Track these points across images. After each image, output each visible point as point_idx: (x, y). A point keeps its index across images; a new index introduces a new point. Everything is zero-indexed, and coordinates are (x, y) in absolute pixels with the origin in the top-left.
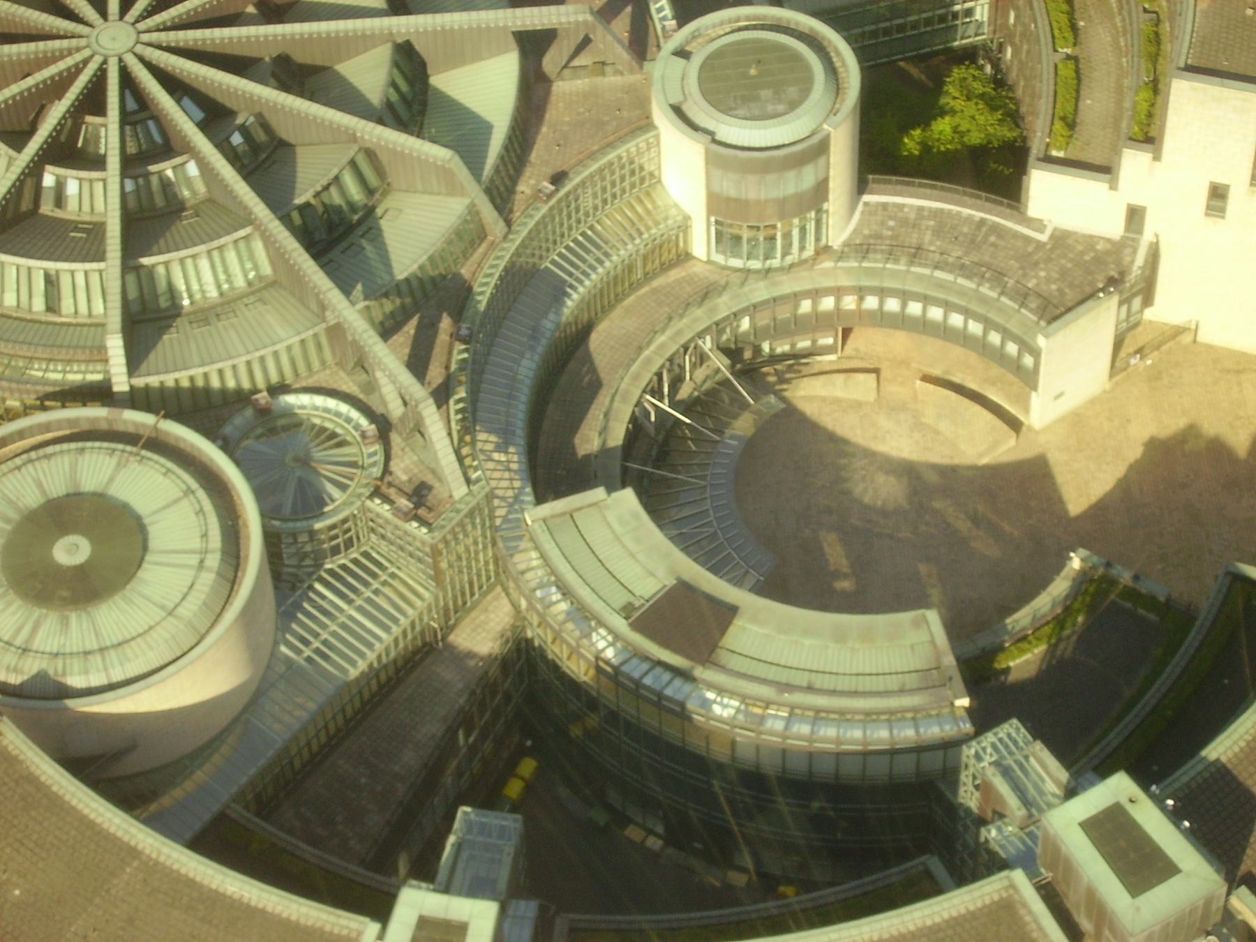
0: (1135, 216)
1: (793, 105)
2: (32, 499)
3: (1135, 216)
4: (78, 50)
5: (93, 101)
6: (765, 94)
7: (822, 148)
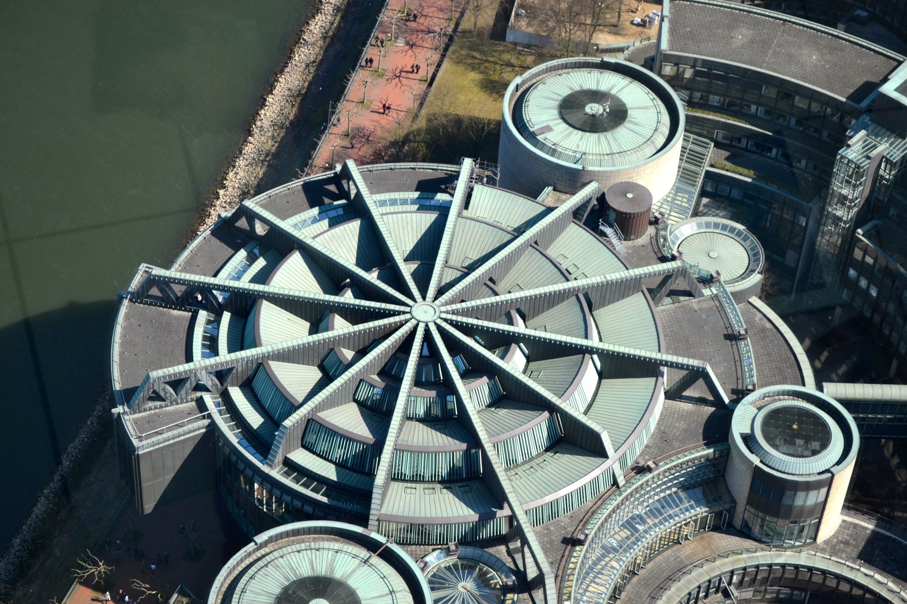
1: (815, 453)
2: (305, 571)
4: (404, 313)
5: (406, 346)
6: (799, 442)
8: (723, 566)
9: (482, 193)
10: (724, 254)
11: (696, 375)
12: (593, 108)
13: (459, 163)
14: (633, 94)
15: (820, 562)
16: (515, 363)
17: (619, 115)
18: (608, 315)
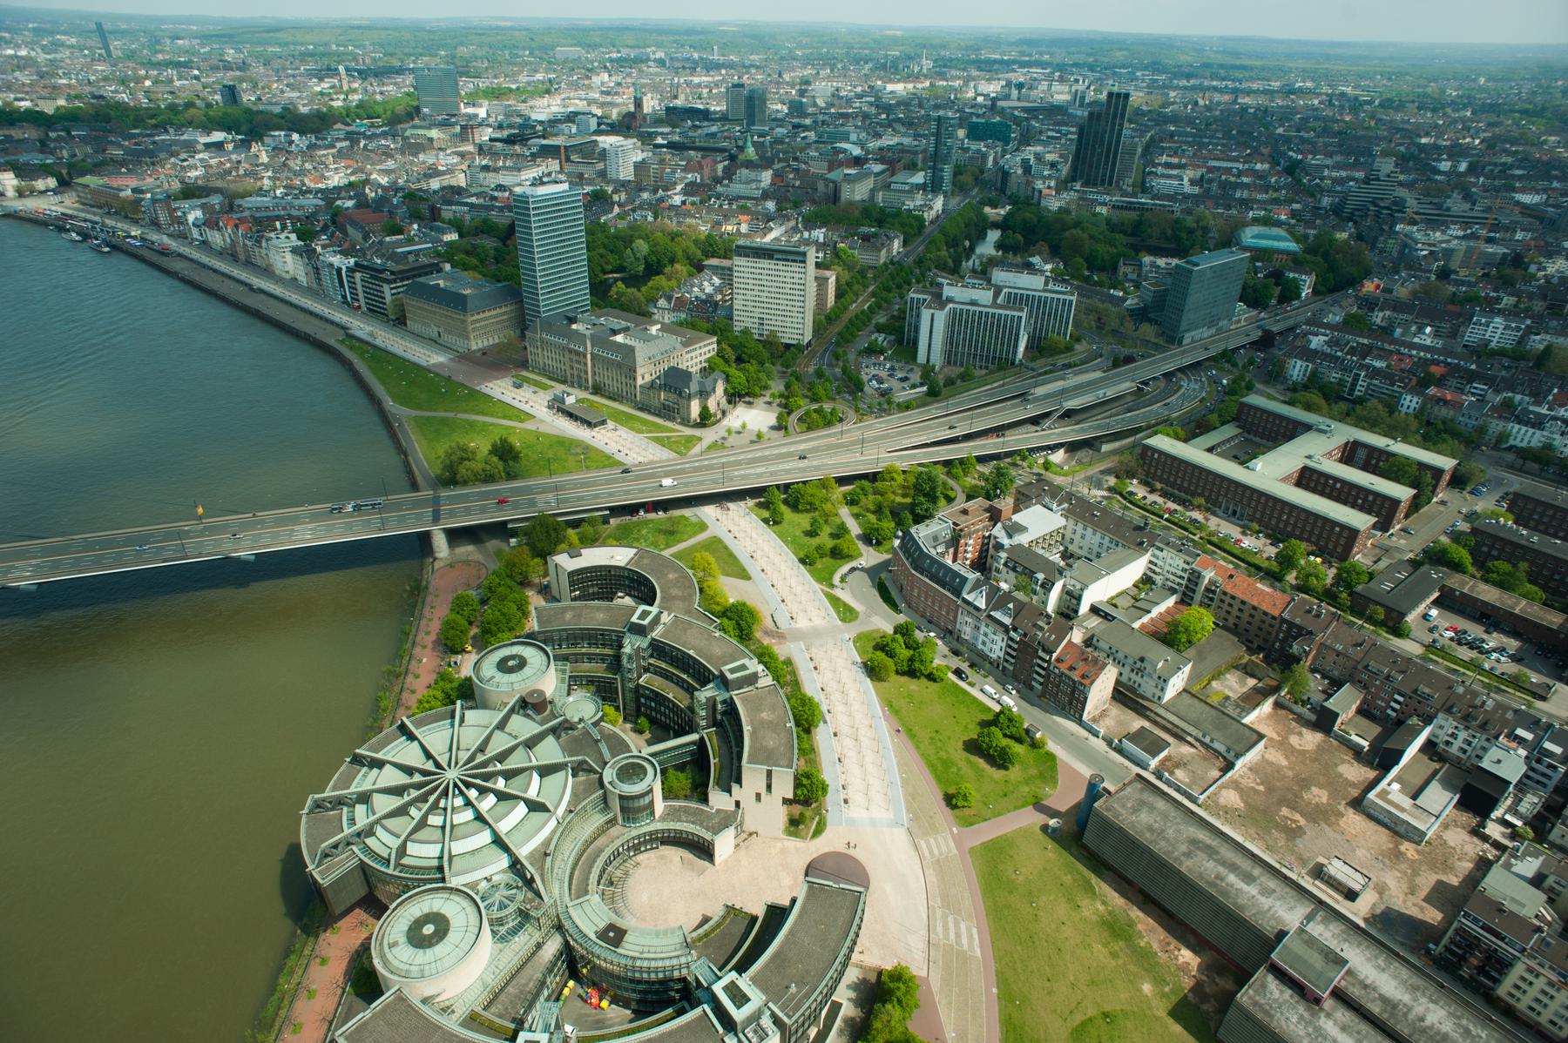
0: (738, 804)
2: (418, 914)
3: (738, 804)
7: (651, 791)
8: (618, 843)
9: (469, 714)
10: (581, 707)
11: (581, 763)
12: (511, 663)
13: (454, 703)
14: (528, 652)
15: (659, 826)
16: (500, 784)
17: (522, 663)
18: (539, 748)
